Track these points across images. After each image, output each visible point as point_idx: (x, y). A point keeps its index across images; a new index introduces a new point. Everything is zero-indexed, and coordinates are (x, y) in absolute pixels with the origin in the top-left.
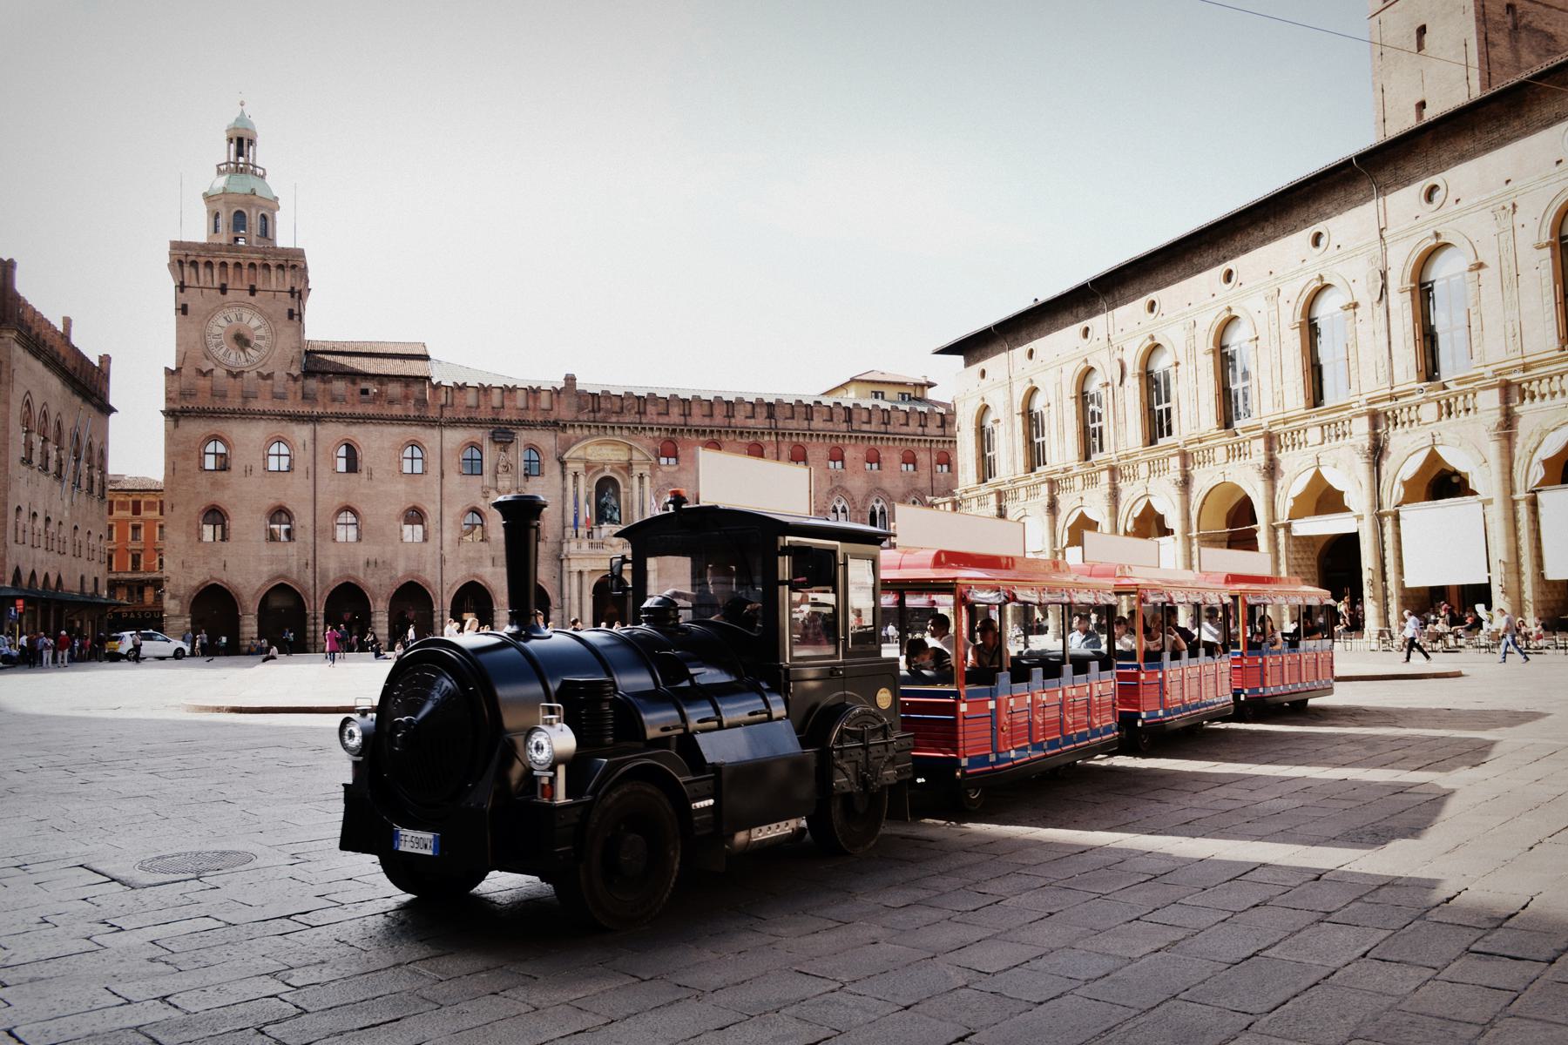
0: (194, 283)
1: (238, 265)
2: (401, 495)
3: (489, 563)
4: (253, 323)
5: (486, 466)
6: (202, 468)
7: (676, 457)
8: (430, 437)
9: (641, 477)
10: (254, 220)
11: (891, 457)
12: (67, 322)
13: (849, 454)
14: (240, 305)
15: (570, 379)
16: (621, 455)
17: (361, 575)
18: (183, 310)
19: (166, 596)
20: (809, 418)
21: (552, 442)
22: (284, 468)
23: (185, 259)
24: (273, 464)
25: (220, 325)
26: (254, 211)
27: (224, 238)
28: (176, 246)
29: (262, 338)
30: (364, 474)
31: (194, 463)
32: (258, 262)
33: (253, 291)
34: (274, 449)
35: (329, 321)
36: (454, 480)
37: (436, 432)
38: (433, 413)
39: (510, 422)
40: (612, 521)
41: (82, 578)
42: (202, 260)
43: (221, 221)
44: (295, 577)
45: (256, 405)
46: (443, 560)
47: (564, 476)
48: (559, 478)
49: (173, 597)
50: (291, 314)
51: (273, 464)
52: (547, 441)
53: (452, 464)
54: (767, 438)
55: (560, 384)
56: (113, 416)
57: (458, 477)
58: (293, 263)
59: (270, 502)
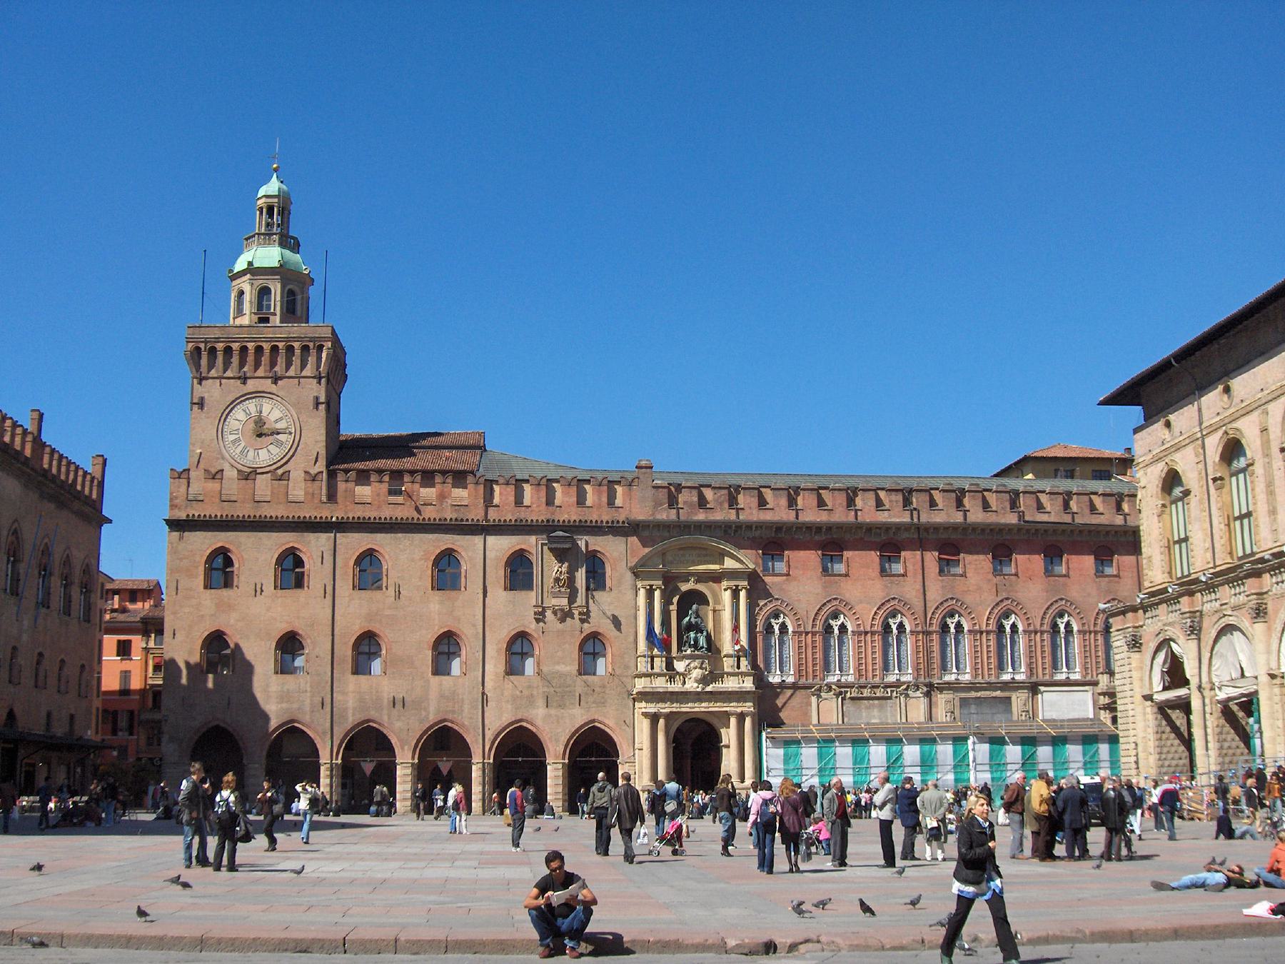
2: (436, 612)
3: (541, 702)
4: (273, 413)
5: (536, 580)
8: (469, 549)
17: (385, 718)
26: (279, 286)
31: (200, 580)
32: (281, 345)
33: (276, 380)
36: (499, 596)
37: (478, 540)
38: (476, 514)
40: (696, 646)
41: (49, 715)
43: (247, 297)
44: (307, 718)
48: (630, 594)
53: (497, 574)
56: (105, 528)
57: (504, 593)
59: (281, 628)
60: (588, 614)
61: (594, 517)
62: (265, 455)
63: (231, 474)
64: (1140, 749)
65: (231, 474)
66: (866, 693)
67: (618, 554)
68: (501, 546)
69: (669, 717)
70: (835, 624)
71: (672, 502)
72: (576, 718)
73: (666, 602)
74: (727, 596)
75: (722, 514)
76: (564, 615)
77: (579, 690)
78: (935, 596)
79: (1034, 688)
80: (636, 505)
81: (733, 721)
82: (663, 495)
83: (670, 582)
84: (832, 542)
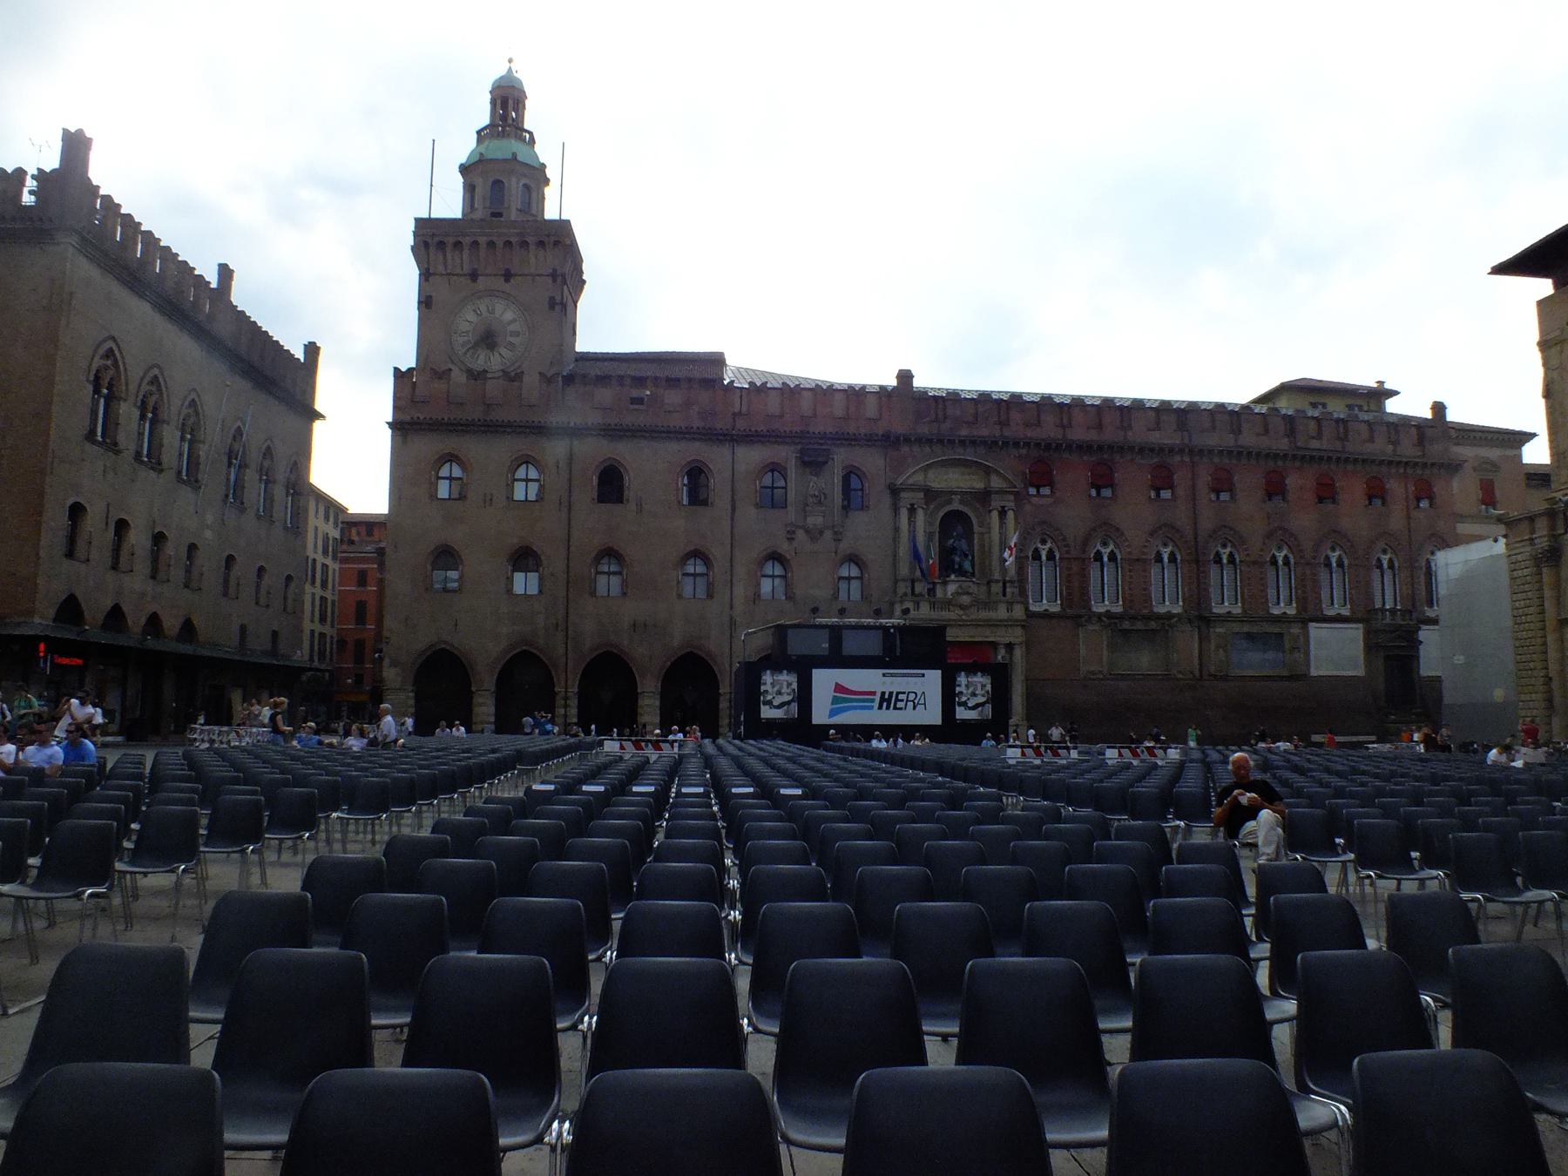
0: (441, 269)
1: (491, 244)
4: (506, 314)
6: (433, 496)
7: (1051, 484)
8: (718, 459)
9: (1003, 513)
10: (514, 187)
11: (1352, 490)
12: (225, 273)
13: (1292, 481)
14: (491, 293)
15: (905, 377)
16: (979, 485)
17: (626, 642)
18: (425, 303)
19: (386, 662)
20: (1237, 431)
21: (881, 463)
22: (532, 497)
23: (432, 239)
24: (519, 494)
25: (468, 320)
27: (478, 215)
28: (418, 221)
29: (517, 334)
30: (632, 506)
32: (513, 240)
33: (508, 276)
34: (521, 473)
35: (608, 324)
36: (749, 516)
37: (725, 451)
38: (721, 425)
39: (824, 436)
40: (961, 572)
41: (243, 629)
42: (450, 240)
45: (499, 415)
46: (732, 623)
47: (896, 510)
49: (394, 664)
50: (552, 304)
51: (519, 493)
52: (872, 462)
54: (1178, 458)
55: (892, 382)
57: (753, 511)
58: (560, 239)
61: (852, 430)
62: (494, 362)
63: (458, 376)
64: (1555, 685)
65: (458, 376)
66: (1139, 625)
68: (750, 457)
70: (1106, 552)
78: (1207, 523)
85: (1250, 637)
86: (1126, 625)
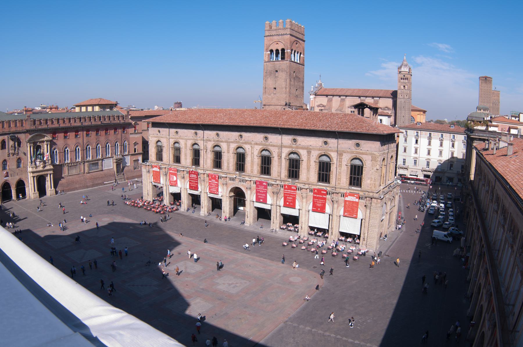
60: (18, 153)
67: (23, 137)
69: (36, 176)
71: (34, 124)
72: (16, 178)
73: (34, 149)
74: (46, 146)
75: (44, 126)
76: (13, 154)
77: (17, 172)
79: (102, 160)
80: (28, 126)
81: (49, 175)
82: (32, 123)
83: (35, 143)
84: (65, 131)
85: (93, 164)
86: (70, 165)
